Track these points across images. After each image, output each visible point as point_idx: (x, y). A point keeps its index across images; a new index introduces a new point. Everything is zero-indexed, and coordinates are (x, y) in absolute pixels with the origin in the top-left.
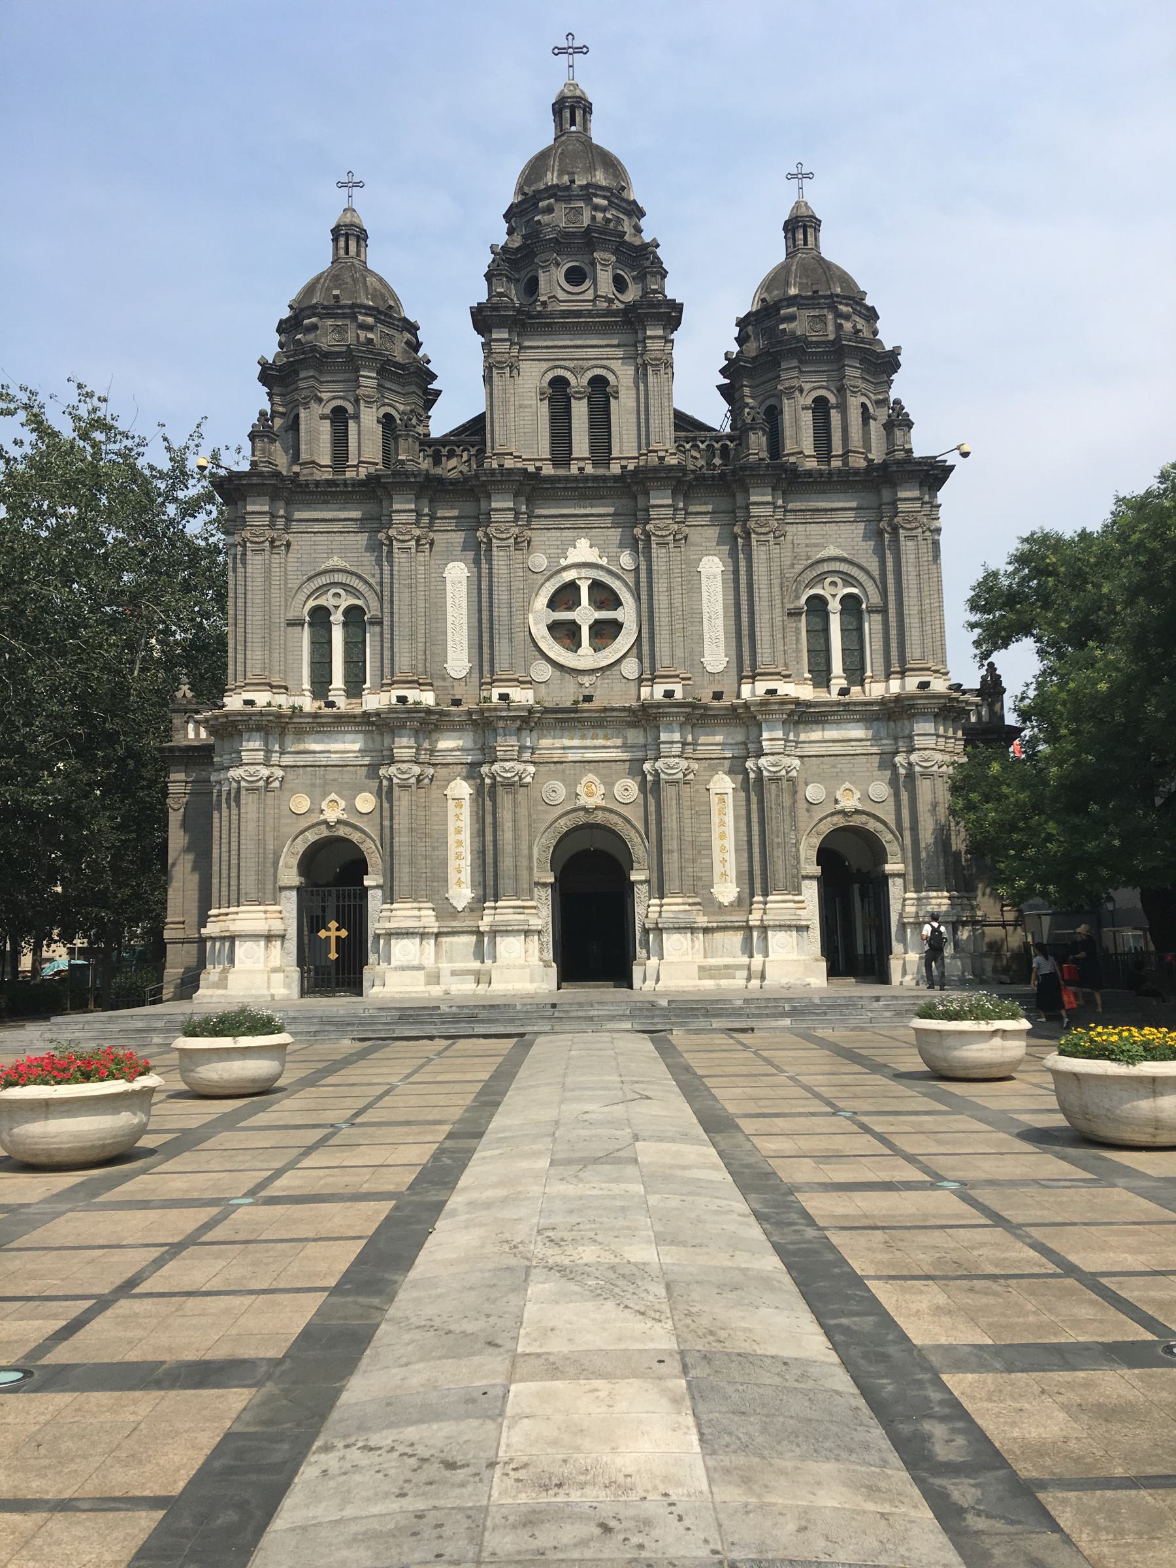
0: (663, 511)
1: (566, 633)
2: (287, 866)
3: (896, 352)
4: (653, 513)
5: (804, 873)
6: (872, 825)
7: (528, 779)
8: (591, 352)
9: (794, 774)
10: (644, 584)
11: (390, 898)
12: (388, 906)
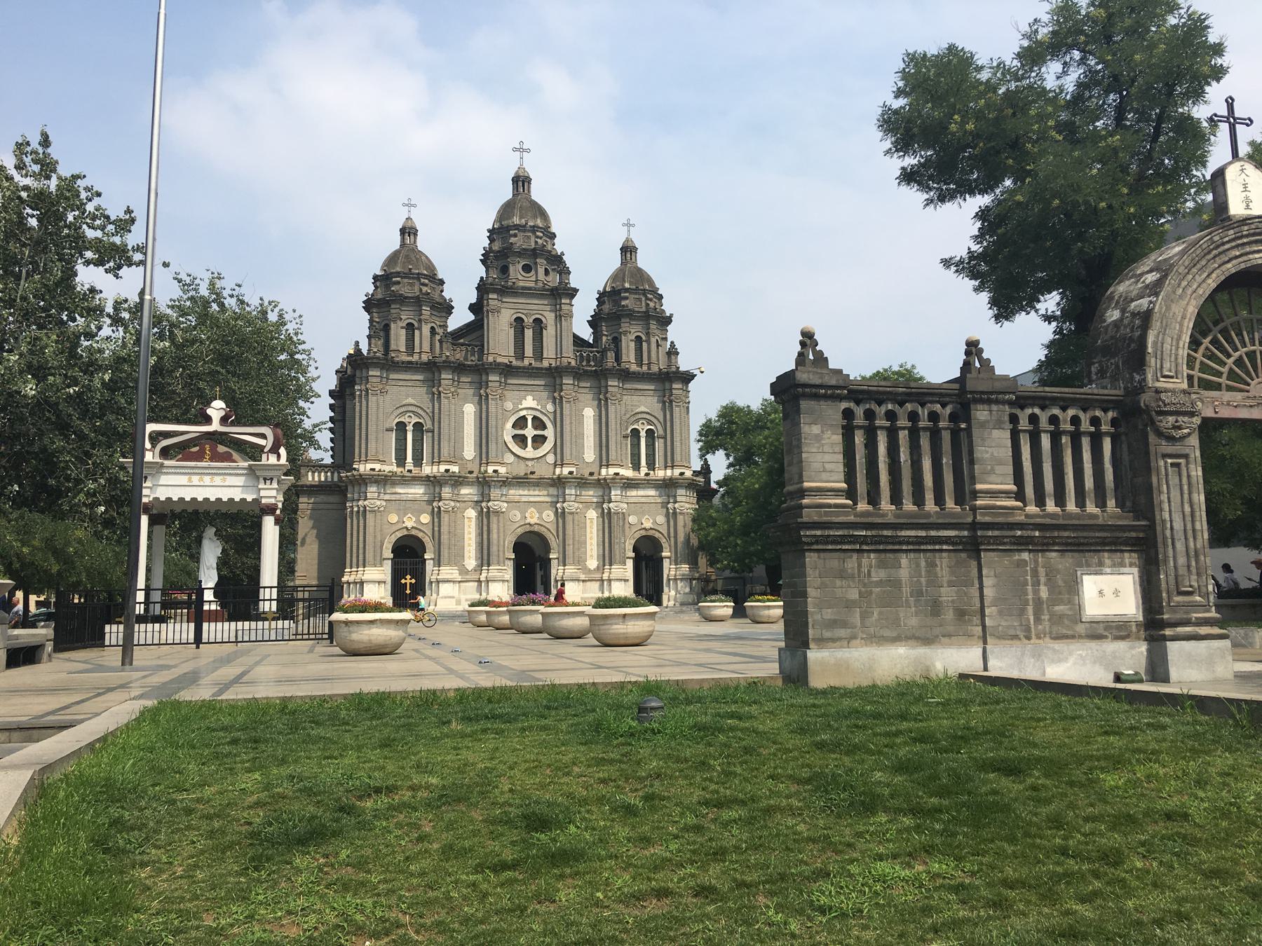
1: (521, 440)
3: (671, 315)
4: (564, 387)
6: (657, 535)
10: (558, 420)
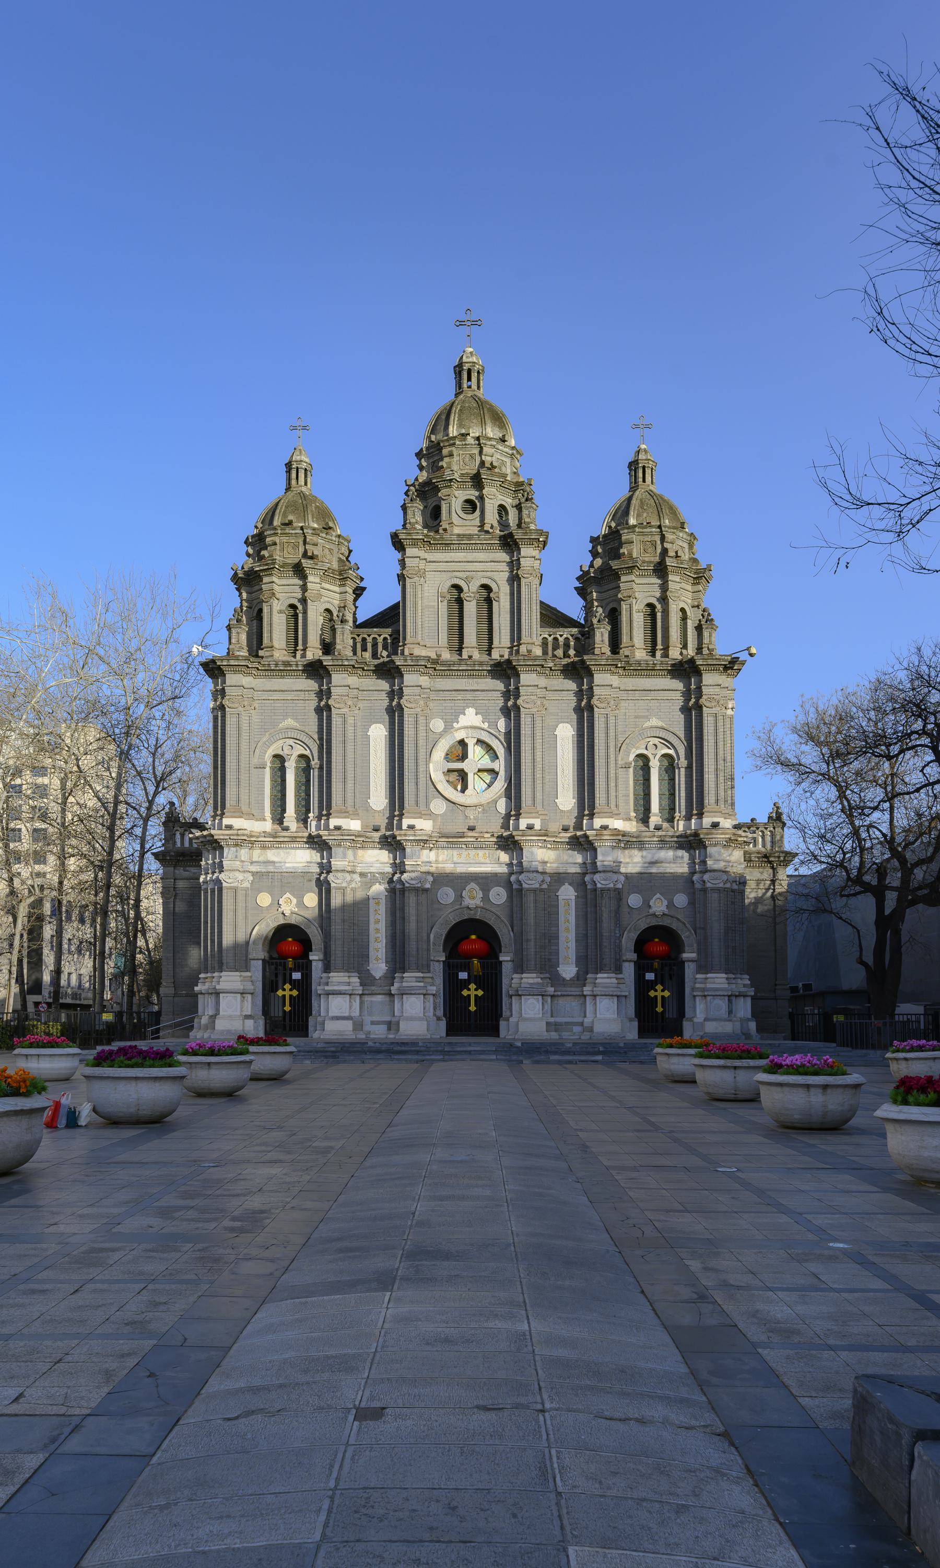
5: (624, 958)
6: (674, 926)
7: (428, 886)
9: (621, 887)
11: (327, 968)
12: (325, 975)
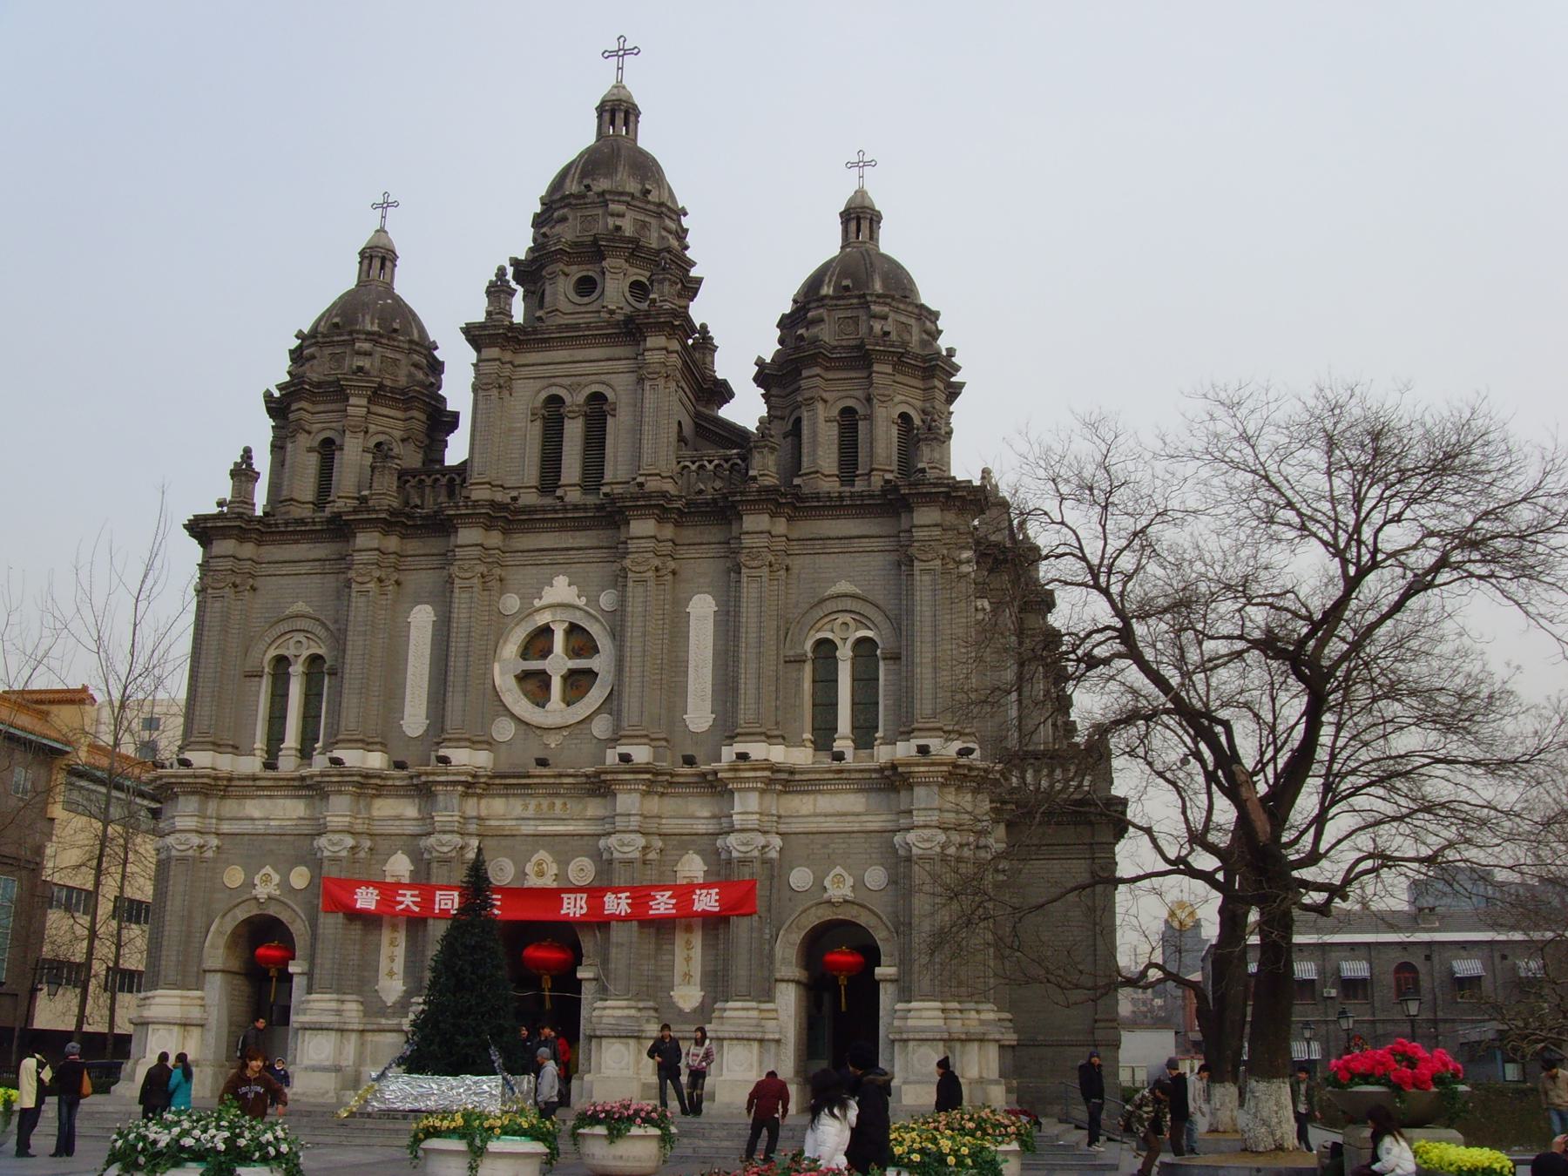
0: (644, 543)
2: (212, 946)
5: (778, 976)
6: (864, 919)
8: (589, 368)
9: (774, 854)
11: (310, 991)
